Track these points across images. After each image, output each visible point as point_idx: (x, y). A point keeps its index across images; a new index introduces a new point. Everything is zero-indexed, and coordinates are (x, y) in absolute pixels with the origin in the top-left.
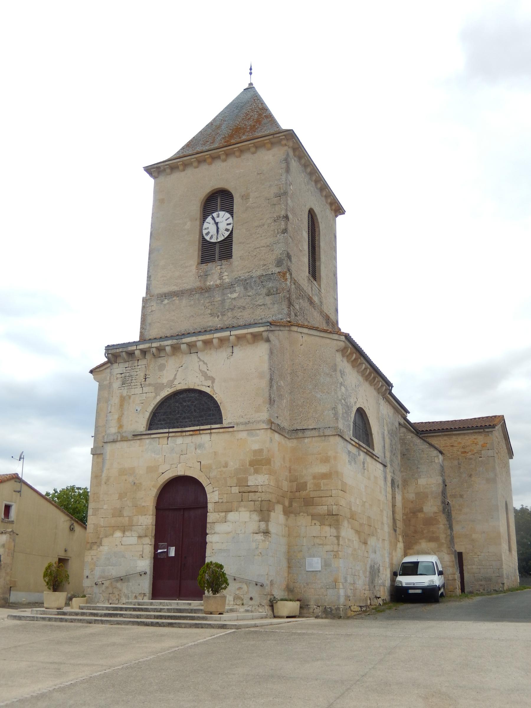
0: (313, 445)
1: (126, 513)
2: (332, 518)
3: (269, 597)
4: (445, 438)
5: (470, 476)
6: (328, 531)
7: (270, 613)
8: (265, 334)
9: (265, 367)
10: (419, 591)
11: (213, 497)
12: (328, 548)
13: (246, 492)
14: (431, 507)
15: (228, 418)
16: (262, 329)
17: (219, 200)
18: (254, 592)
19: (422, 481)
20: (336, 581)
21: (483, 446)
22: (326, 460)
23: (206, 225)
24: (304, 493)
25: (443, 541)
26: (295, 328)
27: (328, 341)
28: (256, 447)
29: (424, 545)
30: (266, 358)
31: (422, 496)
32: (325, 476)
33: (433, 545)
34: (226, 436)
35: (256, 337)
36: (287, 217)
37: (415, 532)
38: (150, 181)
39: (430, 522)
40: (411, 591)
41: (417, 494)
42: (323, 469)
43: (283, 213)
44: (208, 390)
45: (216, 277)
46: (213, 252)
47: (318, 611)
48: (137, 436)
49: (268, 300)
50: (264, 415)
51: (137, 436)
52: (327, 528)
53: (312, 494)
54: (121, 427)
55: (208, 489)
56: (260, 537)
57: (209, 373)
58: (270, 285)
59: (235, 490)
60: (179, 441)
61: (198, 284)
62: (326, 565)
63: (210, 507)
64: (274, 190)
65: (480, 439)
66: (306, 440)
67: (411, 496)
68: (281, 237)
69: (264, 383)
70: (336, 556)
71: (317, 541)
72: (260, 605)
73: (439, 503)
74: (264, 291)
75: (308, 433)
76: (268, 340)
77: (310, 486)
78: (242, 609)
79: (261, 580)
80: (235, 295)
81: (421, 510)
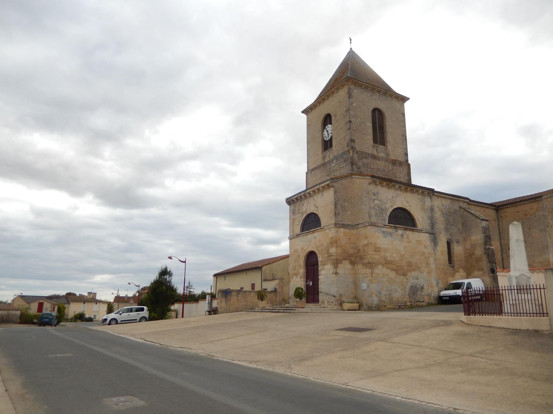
0: (362, 231)
1: (297, 268)
2: (371, 265)
3: (339, 302)
4: (514, 208)
5: (530, 229)
6: (368, 271)
7: (340, 308)
8: (330, 184)
9: (333, 199)
10: (448, 298)
11: (320, 259)
12: (369, 278)
13: (330, 255)
14: (479, 252)
15: (323, 224)
16: (329, 182)
17: (327, 119)
18: (333, 299)
19: (473, 238)
20: (372, 294)
21: (537, 210)
22: (366, 238)
23: (324, 133)
24: (360, 254)
25: (486, 270)
26: (353, 176)
27: (365, 180)
28: (331, 236)
29: (476, 273)
30: (333, 194)
31: (474, 246)
32: (366, 245)
33: (480, 273)
34: (323, 232)
35: (328, 186)
36: (350, 122)
37: (472, 266)
38: (304, 116)
39: (478, 260)
40: (444, 298)
41: (472, 245)
42: (365, 242)
43: (348, 120)
44: (316, 212)
45: (328, 157)
46: (327, 145)
47: (366, 308)
48: (298, 235)
49: (344, 164)
50: (333, 222)
51: (298, 235)
52: (368, 269)
53: (363, 254)
54: (293, 232)
55: (318, 256)
56: (334, 275)
57: (317, 205)
58: (345, 157)
59: (326, 255)
60: (309, 236)
61: (322, 162)
62: (368, 286)
63: (319, 263)
64: (345, 109)
65: (535, 205)
66: (360, 229)
67: (468, 246)
68: (348, 132)
69: (332, 207)
70: (371, 282)
71: (365, 276)
72: (335, 305)
73: (483, 249)
74: (343, 160)
75: (360, 226)
76: (333, 187)
77: (361, 251)
78: (329, 307)
79: (335, 294)
80: (334, 164)
81: (474, 254)
